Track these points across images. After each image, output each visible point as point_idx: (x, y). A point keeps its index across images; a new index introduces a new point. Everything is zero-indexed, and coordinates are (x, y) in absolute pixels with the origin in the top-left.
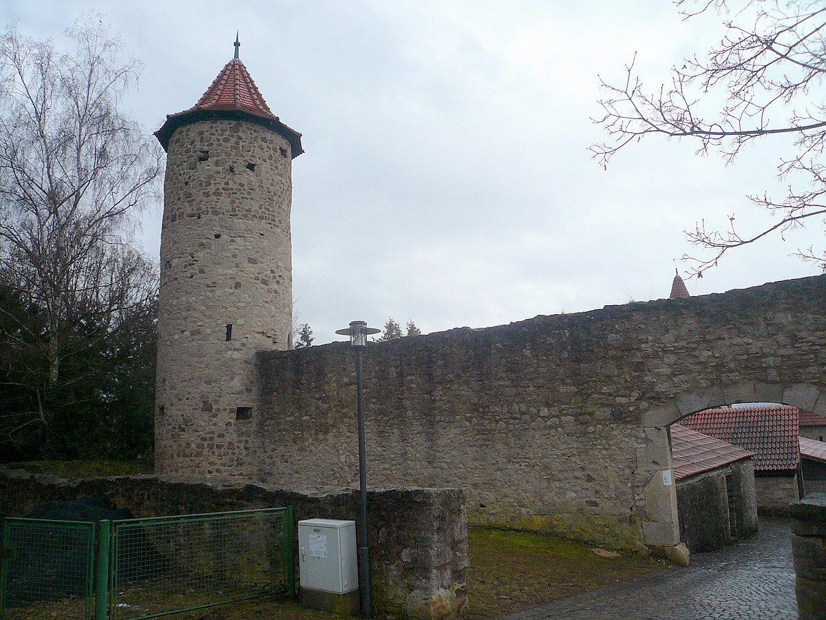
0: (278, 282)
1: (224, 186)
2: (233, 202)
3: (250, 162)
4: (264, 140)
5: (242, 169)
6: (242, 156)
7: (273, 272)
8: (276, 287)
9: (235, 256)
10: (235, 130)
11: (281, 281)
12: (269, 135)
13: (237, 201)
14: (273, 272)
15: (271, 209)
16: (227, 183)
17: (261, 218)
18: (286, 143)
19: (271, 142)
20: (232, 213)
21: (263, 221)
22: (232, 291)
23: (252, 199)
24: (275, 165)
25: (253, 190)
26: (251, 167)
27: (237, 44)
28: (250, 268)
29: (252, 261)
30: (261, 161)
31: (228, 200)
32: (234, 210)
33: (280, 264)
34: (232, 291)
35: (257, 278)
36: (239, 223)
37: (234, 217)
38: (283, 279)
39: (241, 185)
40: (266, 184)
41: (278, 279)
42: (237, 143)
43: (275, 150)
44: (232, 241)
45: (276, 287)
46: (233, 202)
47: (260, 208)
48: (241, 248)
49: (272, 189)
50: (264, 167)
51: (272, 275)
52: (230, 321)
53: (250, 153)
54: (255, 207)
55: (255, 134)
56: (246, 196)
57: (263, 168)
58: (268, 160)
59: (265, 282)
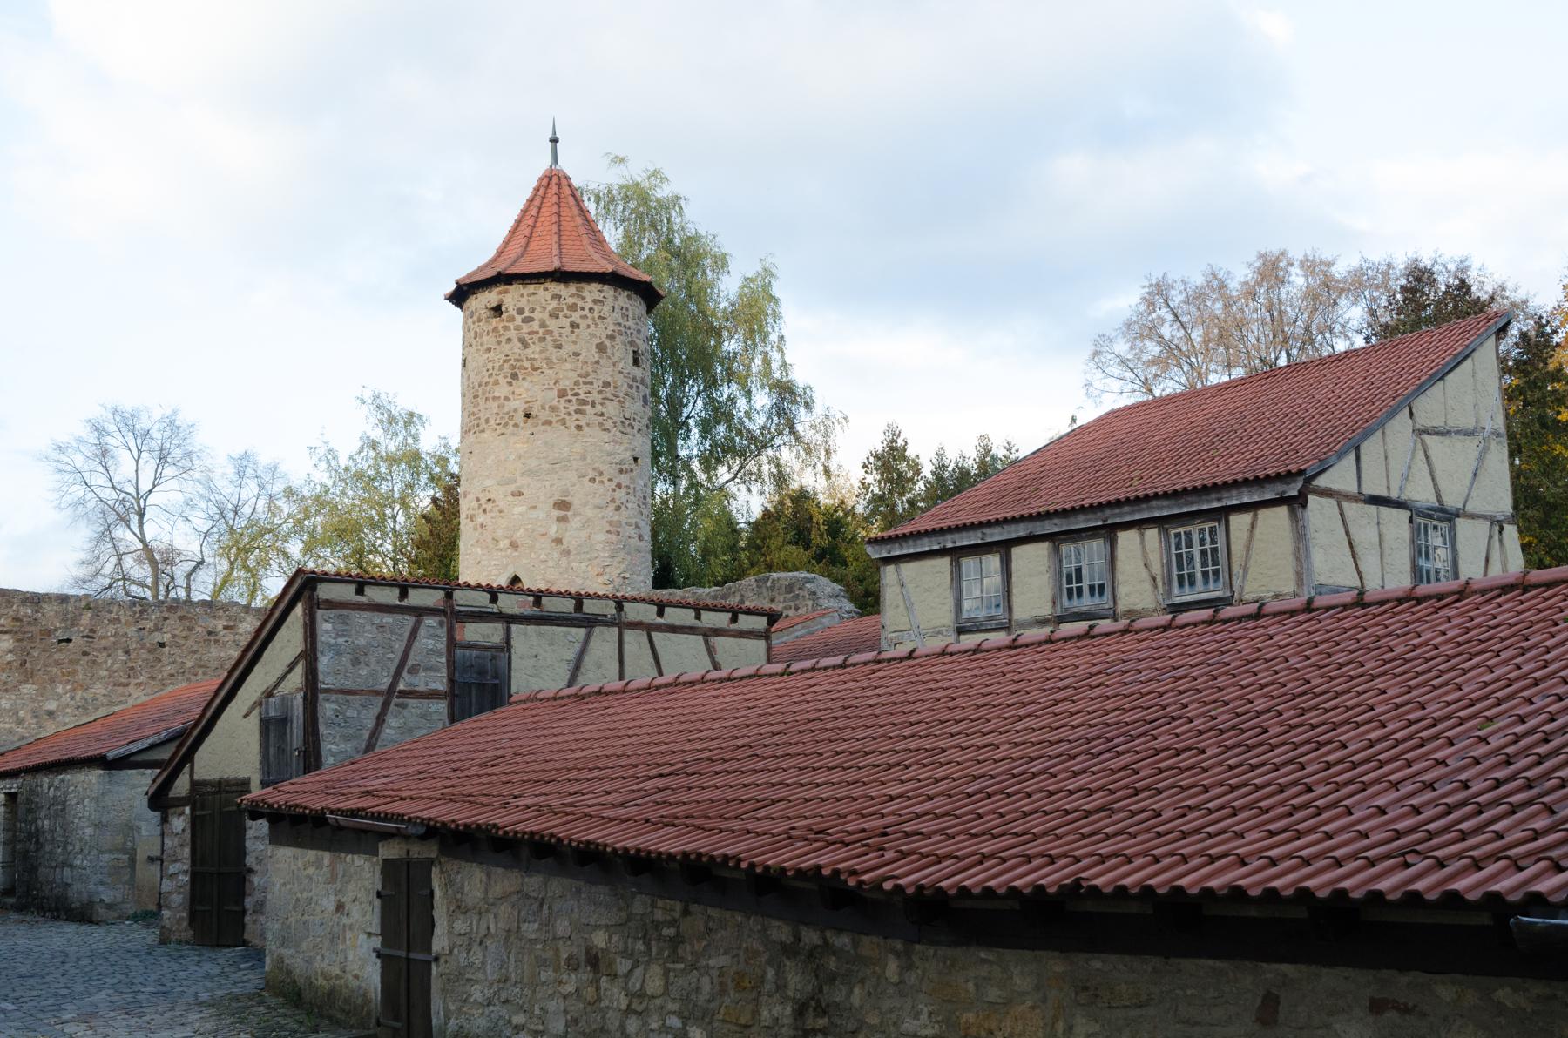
33: (488, 483)
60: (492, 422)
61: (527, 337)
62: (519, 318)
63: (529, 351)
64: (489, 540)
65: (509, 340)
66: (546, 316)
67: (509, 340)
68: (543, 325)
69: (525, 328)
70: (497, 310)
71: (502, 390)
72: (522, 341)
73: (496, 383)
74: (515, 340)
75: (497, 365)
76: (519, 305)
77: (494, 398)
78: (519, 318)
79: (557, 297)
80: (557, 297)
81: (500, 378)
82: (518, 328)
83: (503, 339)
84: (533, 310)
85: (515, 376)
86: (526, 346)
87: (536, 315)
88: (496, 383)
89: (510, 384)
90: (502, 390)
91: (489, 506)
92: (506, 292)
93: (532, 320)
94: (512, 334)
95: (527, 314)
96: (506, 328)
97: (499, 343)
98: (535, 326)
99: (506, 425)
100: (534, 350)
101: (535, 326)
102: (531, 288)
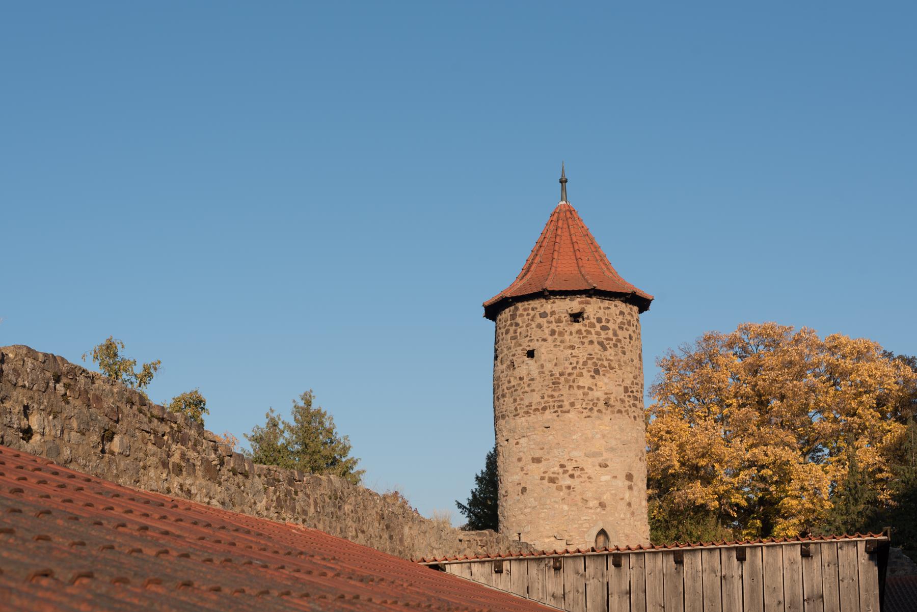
0: (572, 476)
1: (507, 385)
2: (515, 400)
3: (528, 349)
4: (543, 315)
5: (520, 360)
6: (520, 345)
7: (562, 466)
8: (568, 482)
9: (519, 460)
10: (513, 317)
11: (577, 473)
12: (547, 306)
13: (518, 399)
14: (562, 466)
15: (556, 394)
16: (509, 382)
17: (544, 409)
18: (580, 303)
19: (553, 313)
20: (515, 413)
21: (547, 411)
22: (518, 498)
23: (533, 391)
24: (559, 339)
25: (533, 380)
26: (531, 354)
27: (563, 182)
28: (536, 470)
29: (537, 460)
30: (541, 343)
31: (511, 400)
32: (516, 409)
33: (574, 454)
34: (518, 498)
35: (542, 478)
36: (522, 421)
37: (517, 418)
38: (582, 469)
39: (521, 379)
40: (548, 366)
41: (571, 472)
42: (515, 332)
43: (559, 321)
44: (517, 443)
45: (568, 482)
46: (515, 400)
47: (543, 398)
48: (525, 450)
49: (556, 371)
50: (543, 351)
51: (561, 471)
52: (519, 530)
53: (528, 338)
54: (535, 398)
55: (532, 313)
56: (527, 389)
57: (543, 350)
58: (550, 339)
59: (552, 480)
60: (578, 406)
61: (605, 342)
62: (598, 326)
63: (607, 353)
64: (578, 498)
65: (591, 342)
66: (617, 328)
67: (591, 342)
68: (615, 334)
69: (603, 335)
70: (576, 317)
71: (586, 381)
72: (601, 344)
73: (581, 375)
74: (596, 343)
75: (581, 361)
76: (598, 315)
77: (579, 387)
78: (598, 326)
79: (622, 313)
80: (622, 313)
81: (584, 372)
82: (598, 334)
83: (586, 341)
84: (608, 321)
85: (597, 372)
86: (605, 349)
87: (610, 325)
88: (581, 375)
89: (593, 377)
90: (586, 381)
91: (577, 473)
92: (588, 303)
93: (608, 329)
94: (594, 337)
95: (604, 323)
96: (589, 332)
97: (583, 343)
98: (610, 332)
99: (591, 409)
100: (610, 352)
101: (610, 332)
102: (606, 303)
